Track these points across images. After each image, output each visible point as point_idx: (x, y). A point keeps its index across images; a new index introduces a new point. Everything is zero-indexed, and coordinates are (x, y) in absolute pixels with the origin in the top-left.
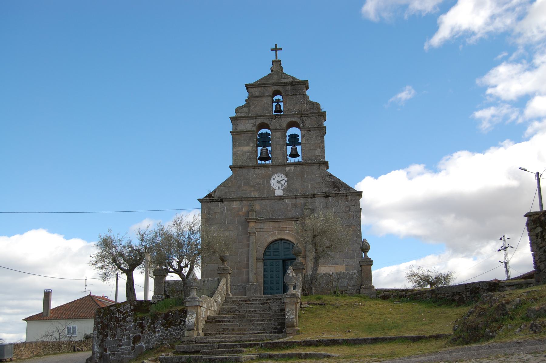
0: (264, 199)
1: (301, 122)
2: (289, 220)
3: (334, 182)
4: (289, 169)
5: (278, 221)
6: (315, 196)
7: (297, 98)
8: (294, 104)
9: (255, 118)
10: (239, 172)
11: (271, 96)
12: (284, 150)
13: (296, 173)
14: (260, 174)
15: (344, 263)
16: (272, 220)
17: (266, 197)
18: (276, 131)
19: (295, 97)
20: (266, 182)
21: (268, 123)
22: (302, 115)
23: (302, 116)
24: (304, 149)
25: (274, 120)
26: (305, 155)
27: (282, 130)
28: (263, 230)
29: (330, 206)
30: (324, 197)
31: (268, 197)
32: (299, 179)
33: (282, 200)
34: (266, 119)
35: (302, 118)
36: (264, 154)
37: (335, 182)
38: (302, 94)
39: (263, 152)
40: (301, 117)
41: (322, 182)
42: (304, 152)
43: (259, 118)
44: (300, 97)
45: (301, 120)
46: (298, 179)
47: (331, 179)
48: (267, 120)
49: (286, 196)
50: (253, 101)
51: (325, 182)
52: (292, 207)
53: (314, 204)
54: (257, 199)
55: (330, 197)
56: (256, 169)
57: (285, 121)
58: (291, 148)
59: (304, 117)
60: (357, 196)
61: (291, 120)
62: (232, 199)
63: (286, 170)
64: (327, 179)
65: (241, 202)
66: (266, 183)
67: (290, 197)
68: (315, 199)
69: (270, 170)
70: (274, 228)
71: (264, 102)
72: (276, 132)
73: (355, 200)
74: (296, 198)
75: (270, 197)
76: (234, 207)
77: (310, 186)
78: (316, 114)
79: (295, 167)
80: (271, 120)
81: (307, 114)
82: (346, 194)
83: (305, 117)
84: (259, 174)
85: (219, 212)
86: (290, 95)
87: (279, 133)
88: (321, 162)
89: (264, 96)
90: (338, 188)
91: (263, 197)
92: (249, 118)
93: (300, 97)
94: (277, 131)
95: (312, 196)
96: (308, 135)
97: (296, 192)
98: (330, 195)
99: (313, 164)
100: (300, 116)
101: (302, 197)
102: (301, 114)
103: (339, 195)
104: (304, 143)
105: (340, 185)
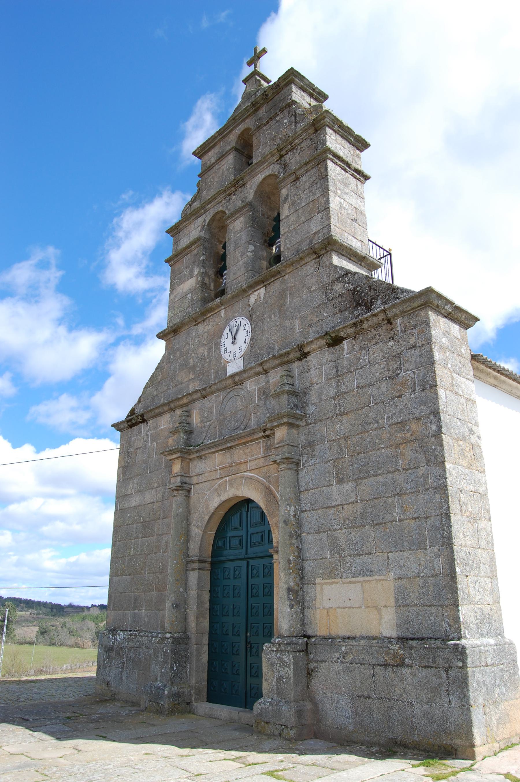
0: (204, 393)
2: (249, 439)
3: (355, 289)
5: (230, 447)
6: (306, 351)
10: (175, 343)
15: (389, 570)
16: (216, 446)
18: (233, 218)
22: (282, 150)
28: (205, 477)
29: (345, 370)
30: (329, 345)
31: (210, 387)
33: (239, 386)
35: (283, 159)
37: (358, 289)
40: (282, 156)
41: (326, 304)
43: (209, 206)
46: (273, 317)
47: (346, 285)
51: (333, 299)
52: (260, 399)
53: (307, 374)
54: (195, 396)
55: (345, 342)
56: (199, 325)
60: (421, 310)
62: (157, 411)
64: (338, 287)
65: (172, 413)
67: (252, 372)
68: (309, 358)
70: (224, 468)
71: (223, 170)
73: (415, 327)
74: (266, 372)
76: (162, 429)
77: (297, 326)
78: (310, 131)
82: (382, 316)
85: (140, 448)
88: (316, 246)
90: (366, 305)
94: (236, 216)
95: (298, 355)
96: (294, 193)
98: (342, 334)
99: (301, 259)
100: (277, 156)
101: (277, 362)
102: (278, 151)
103: (365, 325)
105: (372, 293)
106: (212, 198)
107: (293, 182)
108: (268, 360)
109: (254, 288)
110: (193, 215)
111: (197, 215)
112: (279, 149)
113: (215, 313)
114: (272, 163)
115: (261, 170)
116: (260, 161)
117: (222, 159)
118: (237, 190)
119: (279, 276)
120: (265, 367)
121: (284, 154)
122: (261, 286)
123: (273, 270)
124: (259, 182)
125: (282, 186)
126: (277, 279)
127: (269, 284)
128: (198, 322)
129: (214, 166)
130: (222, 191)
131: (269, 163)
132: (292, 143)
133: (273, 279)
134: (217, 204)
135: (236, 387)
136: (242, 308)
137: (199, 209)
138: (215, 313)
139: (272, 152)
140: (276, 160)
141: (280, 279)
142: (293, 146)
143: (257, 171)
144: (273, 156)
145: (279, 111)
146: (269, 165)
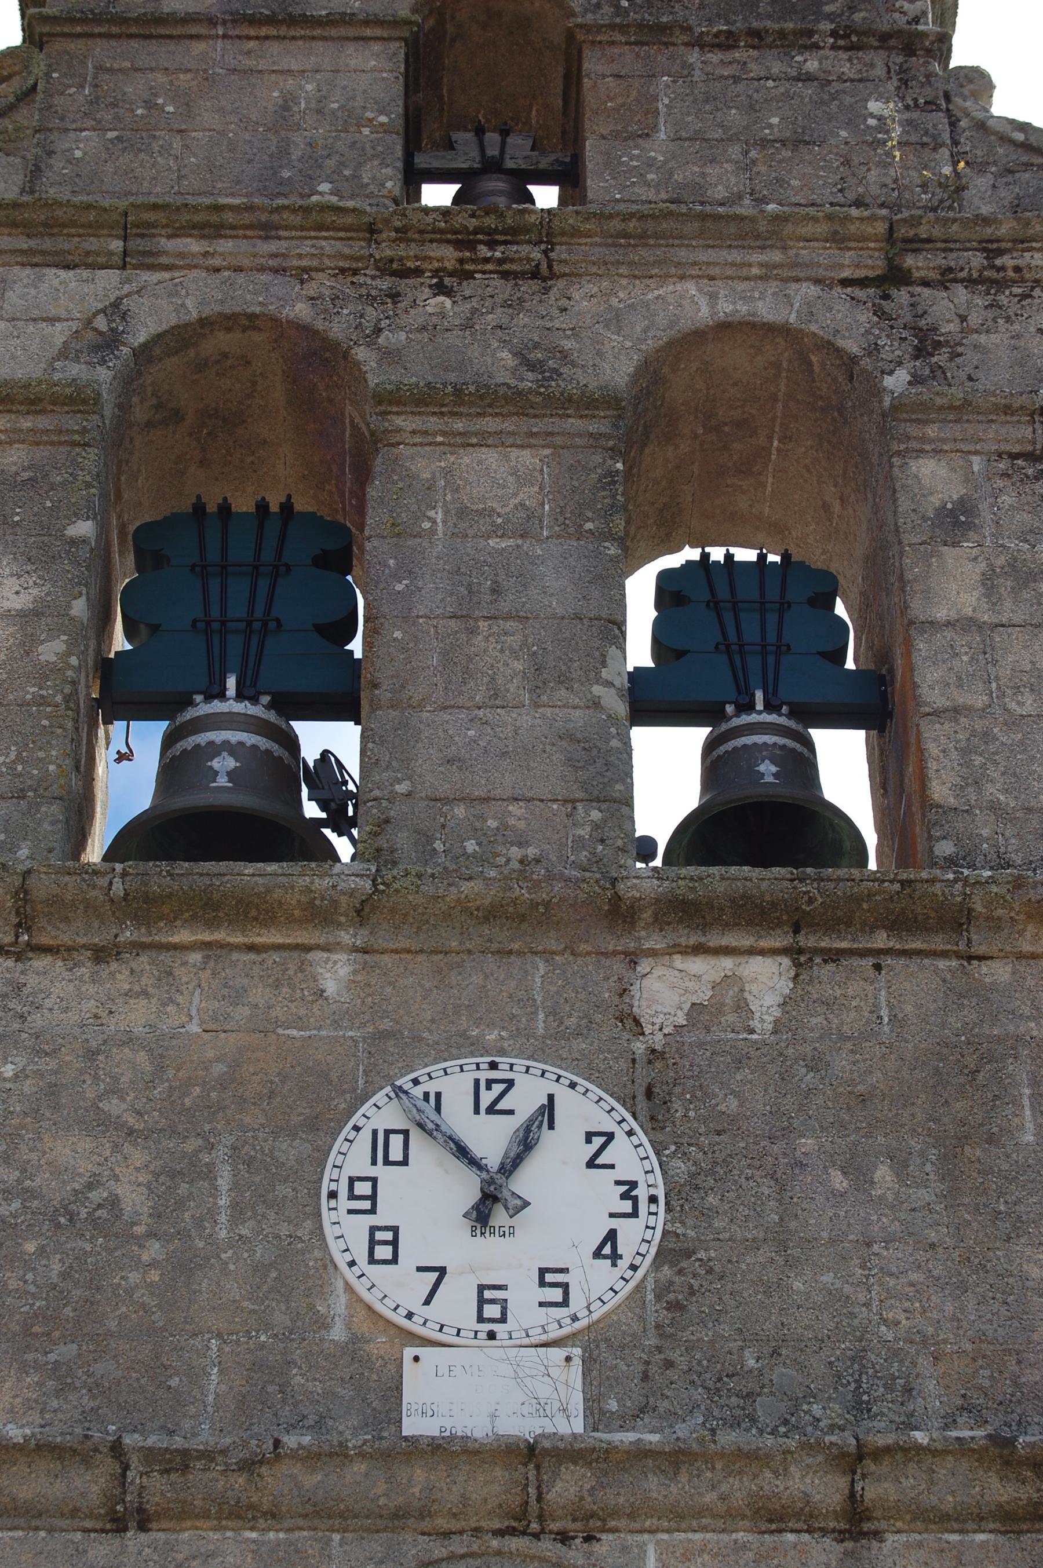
1: (890, 348)
4: (704, 995)
7: (808, 78)
8: (764, 143)
9: (117, 245)
11: (396, 23)
12: (596, 704)
13: (841, 1062)
14: (129, 1040)
17: (208, 1456)
18: (459, 425)
19: (776, 68)
20: (235, 1186)
21: (337, 329)
22: (916, 244)
23: (909, 261)
24: (980, 701)
25: (441, 289)
26: (993, 791)
27: (573, 424)
31: (249, 1466)
32: (901, 1167)
34: (302, 276)
35: (902, 296)
36: (222, 781)
38: (884, 38)
39: (214, 750)
42: (965, 752)
43: (194, 246)
44: (848, 70)
45: (880, 313)
46: (883, 1173)
48: (324, 284)
49: (641, 1453)
50: (100, 68)
57: (615, 320)
58: (709, 747)
59: (946, 279)
61: (725, 308)
63: (642, 1009)
66: (237, 1210)
69: (331, 987)
72: (464, 442)
75: (311, 1458)
79: (825, 971)
80: (394, 296)
81: (991, 250)
83: (961, 293)
84: (91, 1055)
86: (699, 43)
87: (526, 458)
89: (292, 21)
91: (150, 1455)
92: (23, 243)
93: (848, 70)
94: (490, 424)
97: (860, 1408)
100: (874, 264)
104: (965, 624)
106: (247, 218)
107: (1013, 456)
108: (935, 1453)
109: (704, 927)
110: (14, 224)
111: (47, 244)
112: (902, 232)
113: (252, 948)
114: (812, 273)
115: (715, 271)
116: (741, 218)
117: (283, 31)
118: (469, 275)
119: (938, 942)
120: (872, 1491)
121: (916, 274)
122: (764, 944)
123: (937, 888)
124: (686, 325)
125: (923, 439)
126: (919, 953)
127: (832, 956)
128: (44, 940)
129: (197, 37)
130: (349, 220)
131: (794, 265)
132: (1000, 252)
133: (881, 940)
134: (261, 269)
135: (515, 1543)
136: (552, 1013)
137: (92, 216)
138: (252, 948)
139: (848, 218)
140: (846, 274)
141: (942, 964)
142: (1003, 268)
143: (683, 254)
144: (838, 240)
145: (834, 34)
146: (787, 273)
